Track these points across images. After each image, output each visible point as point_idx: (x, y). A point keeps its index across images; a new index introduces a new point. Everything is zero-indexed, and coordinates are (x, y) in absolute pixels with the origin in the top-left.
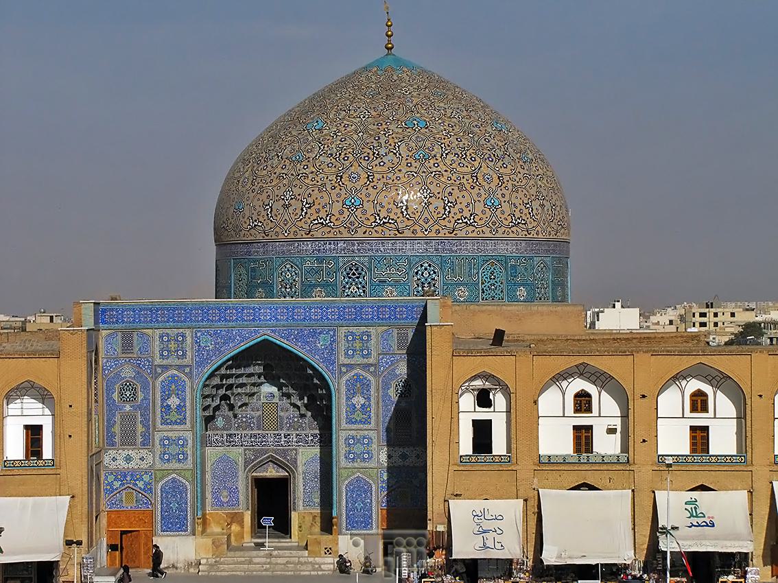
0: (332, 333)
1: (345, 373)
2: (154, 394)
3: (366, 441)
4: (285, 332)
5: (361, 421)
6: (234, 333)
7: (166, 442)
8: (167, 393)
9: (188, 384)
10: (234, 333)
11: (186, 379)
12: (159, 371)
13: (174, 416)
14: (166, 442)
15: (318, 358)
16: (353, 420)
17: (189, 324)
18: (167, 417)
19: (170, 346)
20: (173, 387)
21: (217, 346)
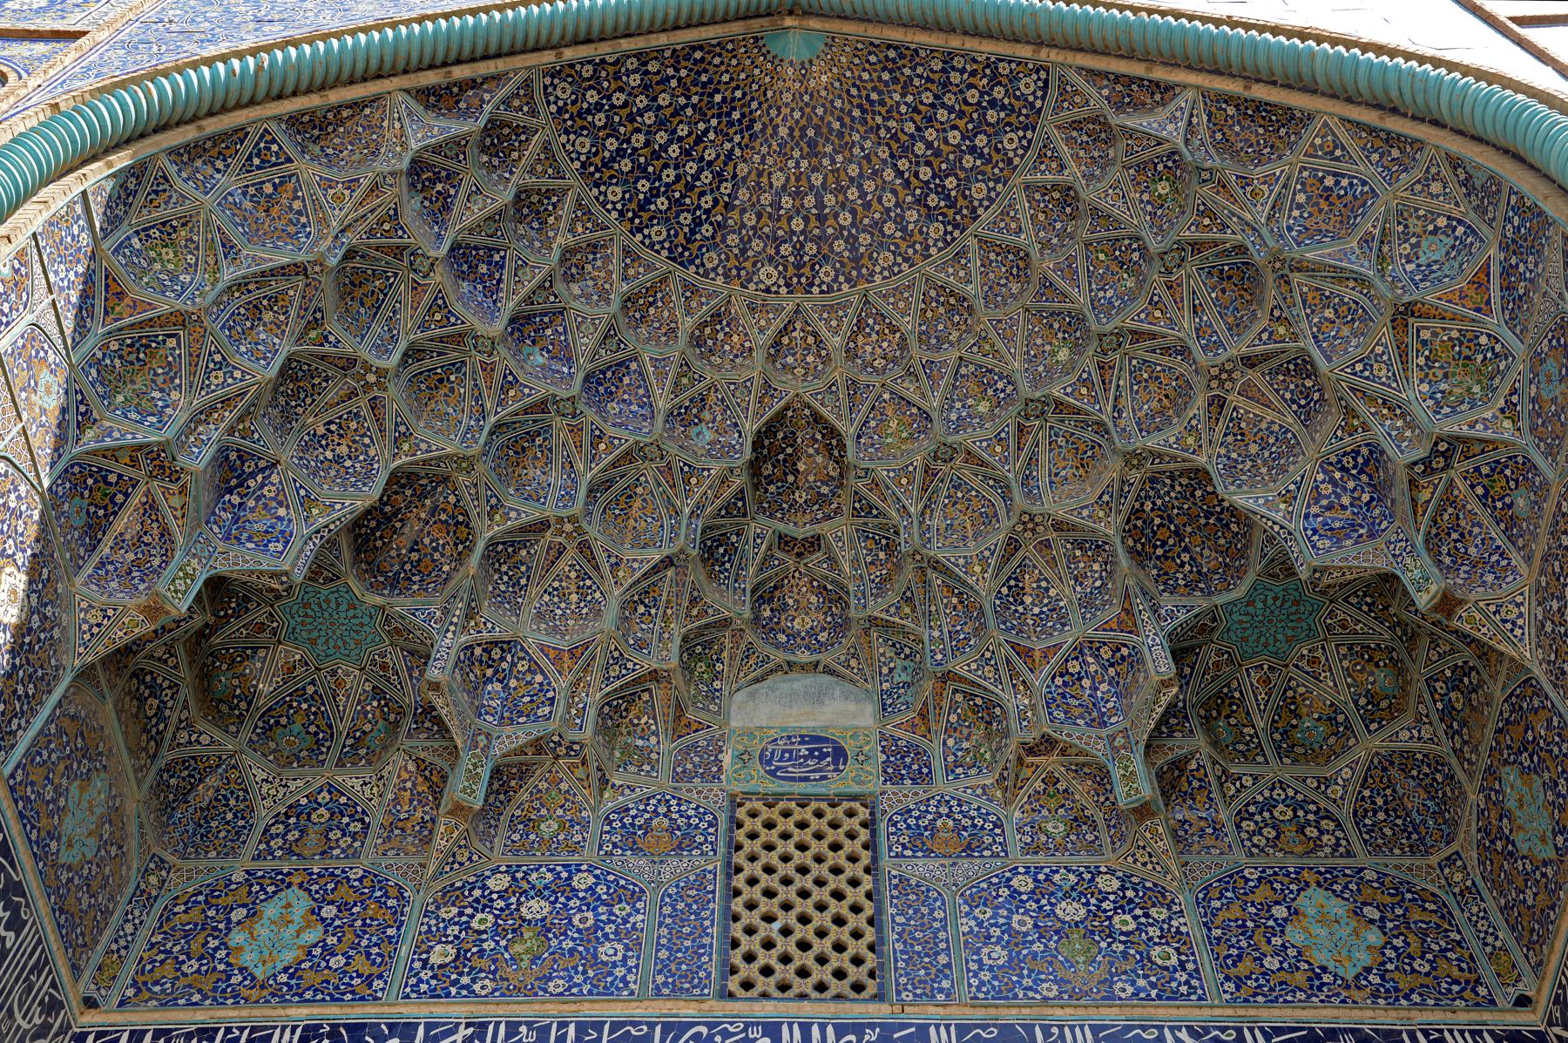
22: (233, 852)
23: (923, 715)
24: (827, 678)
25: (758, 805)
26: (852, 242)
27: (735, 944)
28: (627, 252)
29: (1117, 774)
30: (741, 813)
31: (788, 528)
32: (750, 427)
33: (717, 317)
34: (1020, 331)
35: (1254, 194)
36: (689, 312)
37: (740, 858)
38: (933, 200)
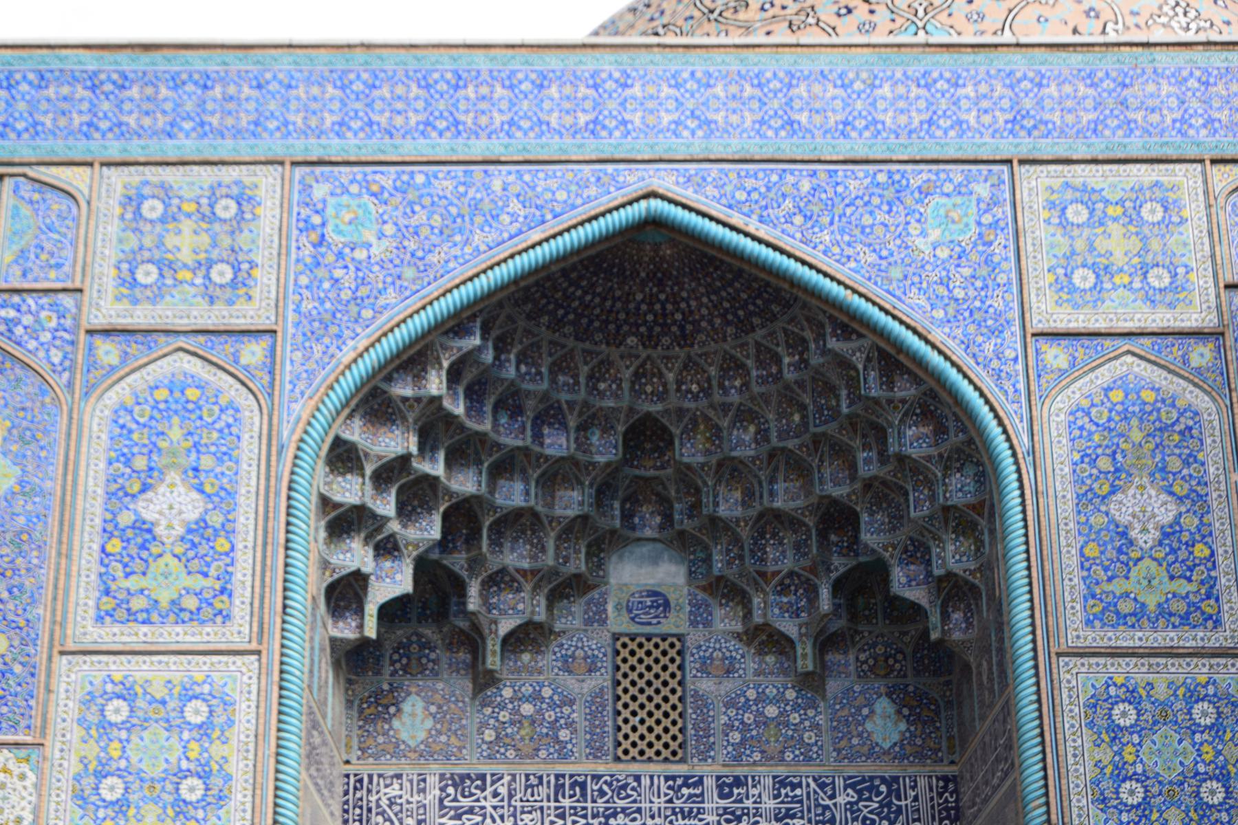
0: (983, 190)
1: (1063, 372)
2: (70, 467)
3: (1203, 713)
4: (749, 183)
5: (1164, 612)
6: (497, 185)
7: (117, 711)
8: (140, 463)
9: (252, 420)
10: (497, 185)
11: (245, 400)
12: (108, 352)
13: (168, 579)
14: (117, 711)
15: (923, 302)
16: (1126, 607)
17: (275, 146)
18: (133, 583)
19: (171, 241)
20: (176, 434)
21: (411, 245)
22: (378, 673)
23: (710, 585)
24: (659, 546)
25: (626, 640)
26: (682, 328)
27: (619, 729)
28: (551, 342)
29: (799, 651)
30: (618, 645)
31: (641, 472)
32: (621, 429)
33: (602, 362)
34: (774, 400)
35: (896, 408)
36: (586, 363)
37: (619, 677)
38: (730, 317)
